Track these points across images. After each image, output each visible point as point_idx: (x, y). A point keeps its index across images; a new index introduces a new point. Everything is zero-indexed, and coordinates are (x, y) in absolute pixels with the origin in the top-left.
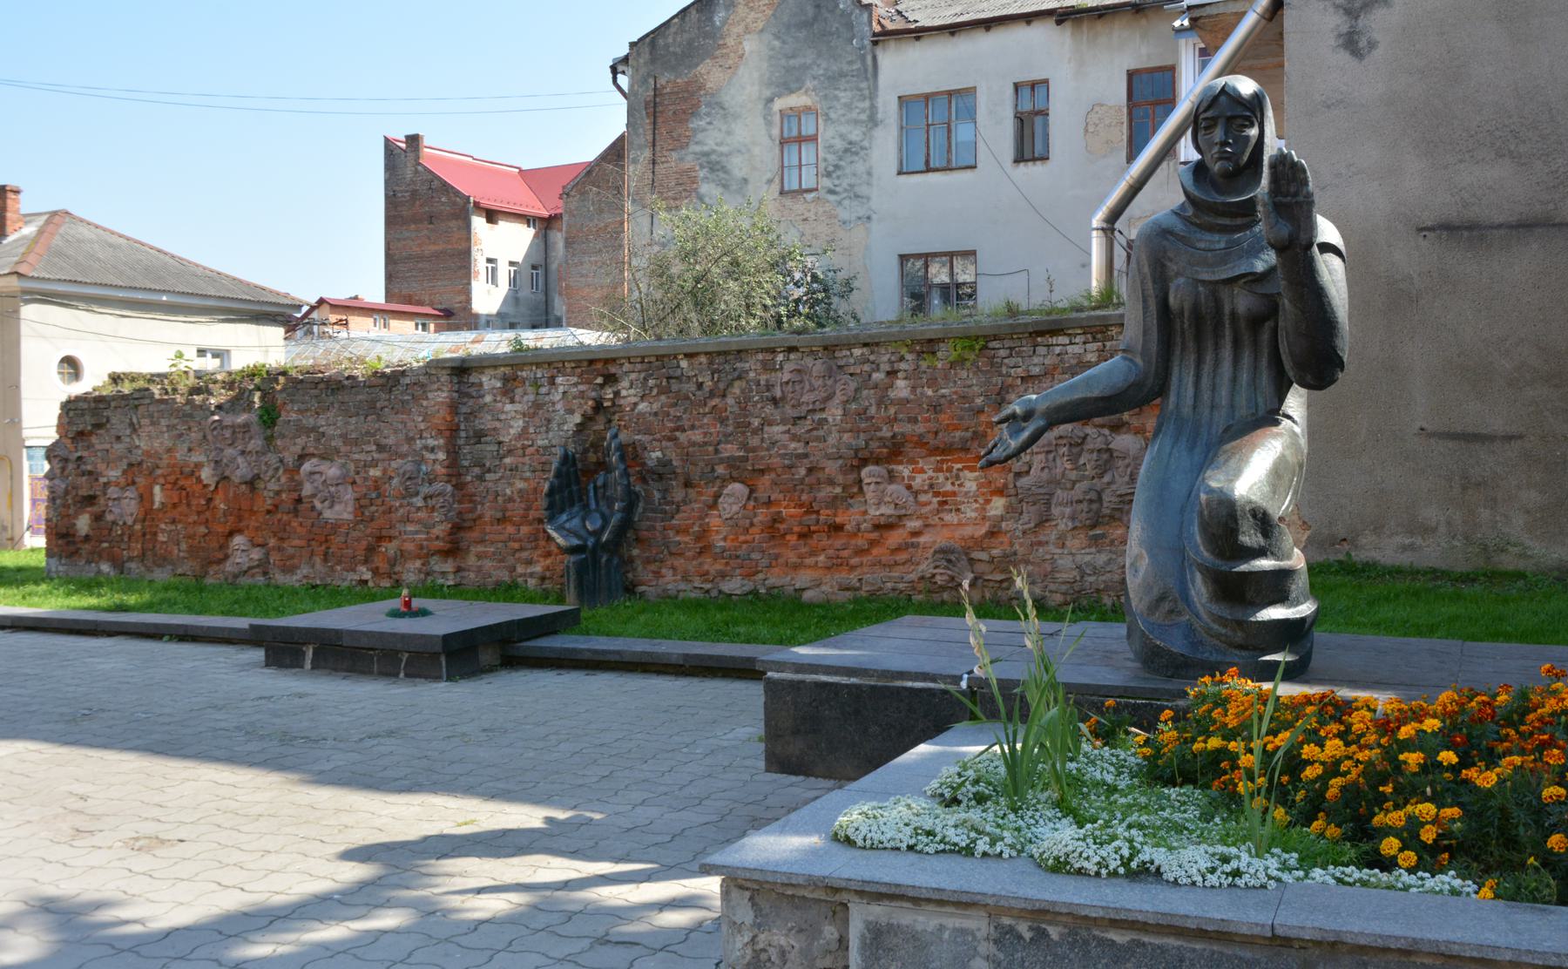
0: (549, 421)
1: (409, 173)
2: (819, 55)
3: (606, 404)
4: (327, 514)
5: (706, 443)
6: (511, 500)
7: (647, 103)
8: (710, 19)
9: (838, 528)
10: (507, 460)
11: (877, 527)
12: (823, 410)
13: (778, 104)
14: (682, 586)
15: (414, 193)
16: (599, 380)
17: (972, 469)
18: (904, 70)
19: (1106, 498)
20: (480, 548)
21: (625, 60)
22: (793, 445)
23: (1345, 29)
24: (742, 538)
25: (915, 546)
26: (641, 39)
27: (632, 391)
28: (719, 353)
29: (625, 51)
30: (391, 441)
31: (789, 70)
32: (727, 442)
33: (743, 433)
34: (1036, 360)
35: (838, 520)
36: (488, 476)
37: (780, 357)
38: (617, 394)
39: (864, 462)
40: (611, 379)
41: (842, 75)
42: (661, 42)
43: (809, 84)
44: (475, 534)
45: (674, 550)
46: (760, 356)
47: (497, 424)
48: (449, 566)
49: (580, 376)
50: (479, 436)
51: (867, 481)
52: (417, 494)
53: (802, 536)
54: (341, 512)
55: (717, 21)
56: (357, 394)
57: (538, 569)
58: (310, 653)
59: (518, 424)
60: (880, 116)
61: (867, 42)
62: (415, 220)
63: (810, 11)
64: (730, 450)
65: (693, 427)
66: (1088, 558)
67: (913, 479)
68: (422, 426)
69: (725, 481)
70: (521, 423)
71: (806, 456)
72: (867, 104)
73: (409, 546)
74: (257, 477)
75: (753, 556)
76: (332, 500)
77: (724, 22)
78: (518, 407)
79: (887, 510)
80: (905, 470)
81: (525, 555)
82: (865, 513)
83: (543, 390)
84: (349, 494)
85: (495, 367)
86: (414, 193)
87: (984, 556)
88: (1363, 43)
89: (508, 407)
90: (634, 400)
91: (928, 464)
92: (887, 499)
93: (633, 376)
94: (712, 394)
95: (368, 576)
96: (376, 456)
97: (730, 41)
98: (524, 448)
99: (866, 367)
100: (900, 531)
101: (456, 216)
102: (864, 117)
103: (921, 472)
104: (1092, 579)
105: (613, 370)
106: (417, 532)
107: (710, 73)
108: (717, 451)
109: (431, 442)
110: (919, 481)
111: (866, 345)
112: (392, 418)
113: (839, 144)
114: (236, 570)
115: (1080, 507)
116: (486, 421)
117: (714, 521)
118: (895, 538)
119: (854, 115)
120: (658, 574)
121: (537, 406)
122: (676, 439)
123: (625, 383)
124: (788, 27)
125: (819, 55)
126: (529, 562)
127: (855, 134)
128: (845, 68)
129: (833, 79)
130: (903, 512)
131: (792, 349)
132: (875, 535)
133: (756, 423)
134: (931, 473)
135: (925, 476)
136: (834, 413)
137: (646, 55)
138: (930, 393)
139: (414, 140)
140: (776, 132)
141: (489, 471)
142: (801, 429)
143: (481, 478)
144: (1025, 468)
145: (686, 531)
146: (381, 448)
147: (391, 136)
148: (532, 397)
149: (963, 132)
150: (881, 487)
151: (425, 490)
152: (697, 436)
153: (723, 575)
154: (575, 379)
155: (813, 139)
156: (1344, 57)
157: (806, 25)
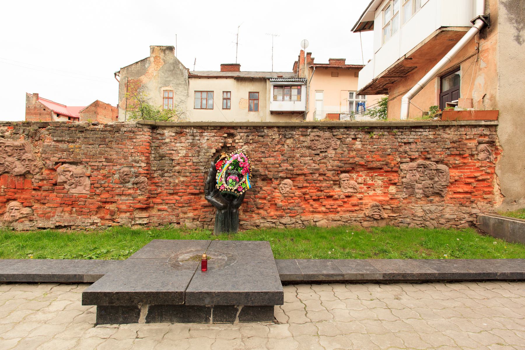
0: (199, 152)
1: (34, 102)
2: (174, 78)
4: (73, 191)
5: (275, 164)
6: (177, 185)
7: (125, 84)
8: (144, 66)
9: (331, 197)
10: (177, 168)
12: (326, 152)
13: (163, 89)
14: (262, 221)
15: (35, 108)
17: (382, 175)
18: (196, 84)
19: (435, 185)
20: (160, 207)
21: (119, 72)
22: (314, 165)
23: (516, 34)
24: (289, 201)
25: (361, 204)
26: (124, 68)
27: (241, 141)
28: (283, 127)
29: (119, 70)
30: (114, 157)
31: (166, 81)
32: (284, 163)
33: (293, 160)
34: (411, 137)
35: (331, 194)
36: (166, 174)
37: (309, 130)
38: (234, 141)
39: (342, 172)
41: (180, 84)
42: (130, 69)
43: (171, 85)
44: (158, 201)
45: (259, 206)
46: (301, 130)
47: (172, 152)
48: (144, 214)
50: (162, 157)
52: (129, 182)
53: (314, 200)
54: (82, 190)
55: (146, 66)
56: (95, 134)
57: (191, 215)
58: (144, 312)
59: (183, 153)
60: (189, 95)
61: (187, 77)
62: (35, 114)
63: (172, 68)
64: (285, 166)
65: (269, 157)
66: (428, 208)
67: (358, 178)
68: (133, 151)
69: (283, 178)
70: (185, 151)
71: (317, 170)
72: (186, 91)
73: (124, 207)
74: (29, 172)
75: (296, 208)
76: (77, 184)
77: (149, 67)
78: (183, 145)
80: (355, 176)
81: (185, 209)
83: (197, 138)
84: (88, 182)
86: (35, 108)
87: (388, 207)
88: (521, 40)
89: (178, 145)
91: (363, 174)
93: (242, 134)
95: (98, 221)
96: (105, 164)
97: (150, 72)
99: (345, 136)
100: (355, 198)
101: (47, 114)
102: (185, 94)
103: (363, 176)
105: (232, 131)
106: (127, 200)
107: (144, 79)
109: (137, 158)
110: (360, 180)
111: (346, 127)
112: (114, 145)
113: (179, 100)
114: (11, 219)
115: (427, 190)
116: (164, 150)
117: (277, 194)
118: (354, 200)
119: (183, 94)
120: (251, 217)
121: (193, 145)
122: (261, 161)
123: (239, 137)
124: (166, 71)
125: (174, 78)
126: (185, 213)
127: (183, 98)
128: (181, 82)
129: (178, 85)
130: (356, 191)
131: (314, 127)
132: (346, 200)
133: (298, 155)
134: (364, 177)
135: (363, 178)
136: (331, 153)
137: (125, 72)
138: (369, 147)
139: (36, 95)
140: (162, 95)
141: (167, 172)
142: (317, 158)
143: (162, 176)
144: (405, 176)
145: (265, 198)
146: (108, 160)
147: (28, 93)
148: (191, 141)
149: (210, 102)
150: (349, 181)
151: (133, 180)
152: (271, 160)
153: (281, 217)
154: (214, 134)
155: (172, 98)
156: (515, 43)
157: (171, 71)
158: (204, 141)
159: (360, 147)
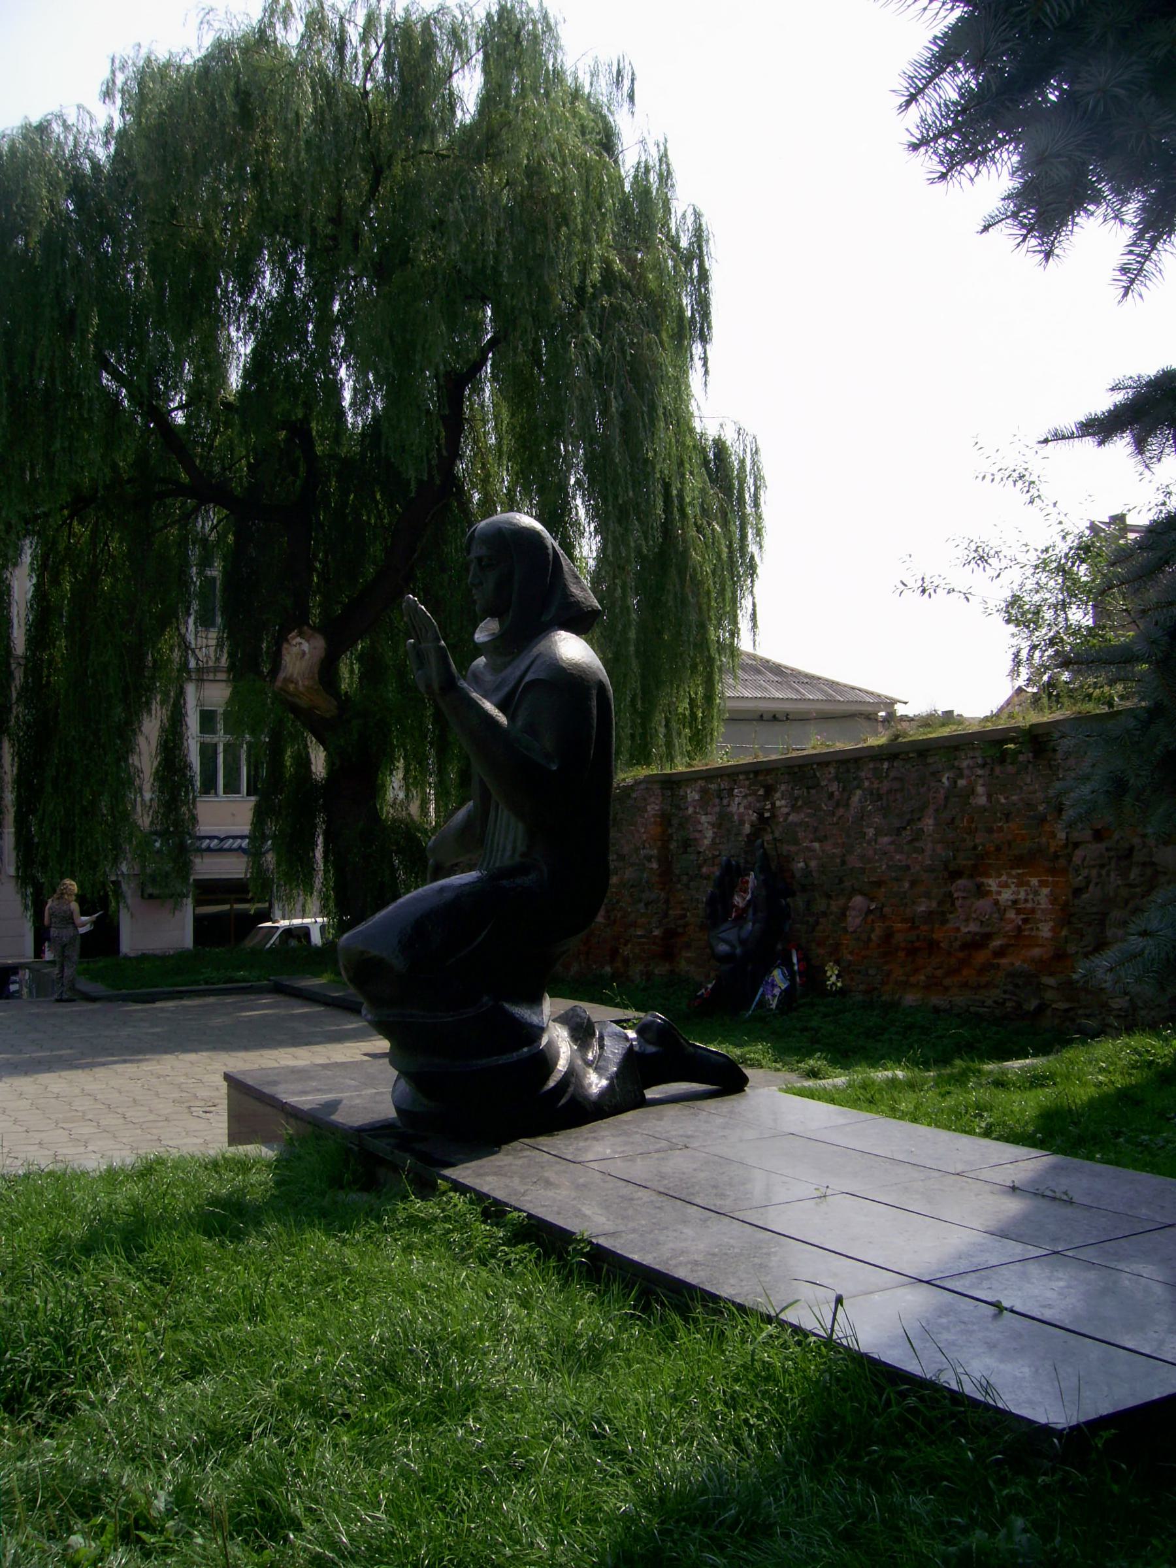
3: (767, 815)
11: (965, 946)
16: (761, 792)
27: (783, 802)
37: (886, 766)
38: (773, 804)
40: (769, 790)
46: (871, 765)
49: (749, 788)
51: (955, 895)
52: (640, 901)
67: (999, 893)
68: (644, 837)
79: (973, 927)
82: (958, 929)
83: (725, 802)
85: (696, 780)
90: (785, 810)
92: (974, 916)
93: (783, 787)
94: (838, 805)
98: (715, 857)
104: (1143, 1013)
105: (770, 780)
108: (843, 863)
118: (981, 957)
123: (778, 795)
130: (988, 930)
148: (717, 809)
158: (734, 809)
159: (982, 801)
